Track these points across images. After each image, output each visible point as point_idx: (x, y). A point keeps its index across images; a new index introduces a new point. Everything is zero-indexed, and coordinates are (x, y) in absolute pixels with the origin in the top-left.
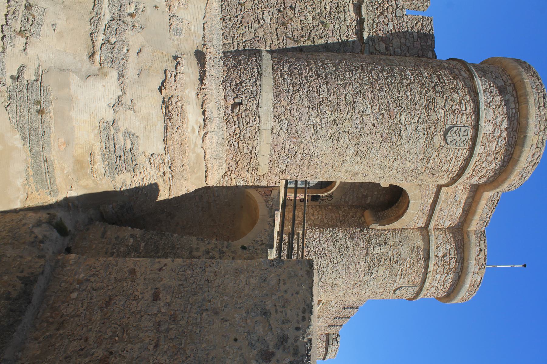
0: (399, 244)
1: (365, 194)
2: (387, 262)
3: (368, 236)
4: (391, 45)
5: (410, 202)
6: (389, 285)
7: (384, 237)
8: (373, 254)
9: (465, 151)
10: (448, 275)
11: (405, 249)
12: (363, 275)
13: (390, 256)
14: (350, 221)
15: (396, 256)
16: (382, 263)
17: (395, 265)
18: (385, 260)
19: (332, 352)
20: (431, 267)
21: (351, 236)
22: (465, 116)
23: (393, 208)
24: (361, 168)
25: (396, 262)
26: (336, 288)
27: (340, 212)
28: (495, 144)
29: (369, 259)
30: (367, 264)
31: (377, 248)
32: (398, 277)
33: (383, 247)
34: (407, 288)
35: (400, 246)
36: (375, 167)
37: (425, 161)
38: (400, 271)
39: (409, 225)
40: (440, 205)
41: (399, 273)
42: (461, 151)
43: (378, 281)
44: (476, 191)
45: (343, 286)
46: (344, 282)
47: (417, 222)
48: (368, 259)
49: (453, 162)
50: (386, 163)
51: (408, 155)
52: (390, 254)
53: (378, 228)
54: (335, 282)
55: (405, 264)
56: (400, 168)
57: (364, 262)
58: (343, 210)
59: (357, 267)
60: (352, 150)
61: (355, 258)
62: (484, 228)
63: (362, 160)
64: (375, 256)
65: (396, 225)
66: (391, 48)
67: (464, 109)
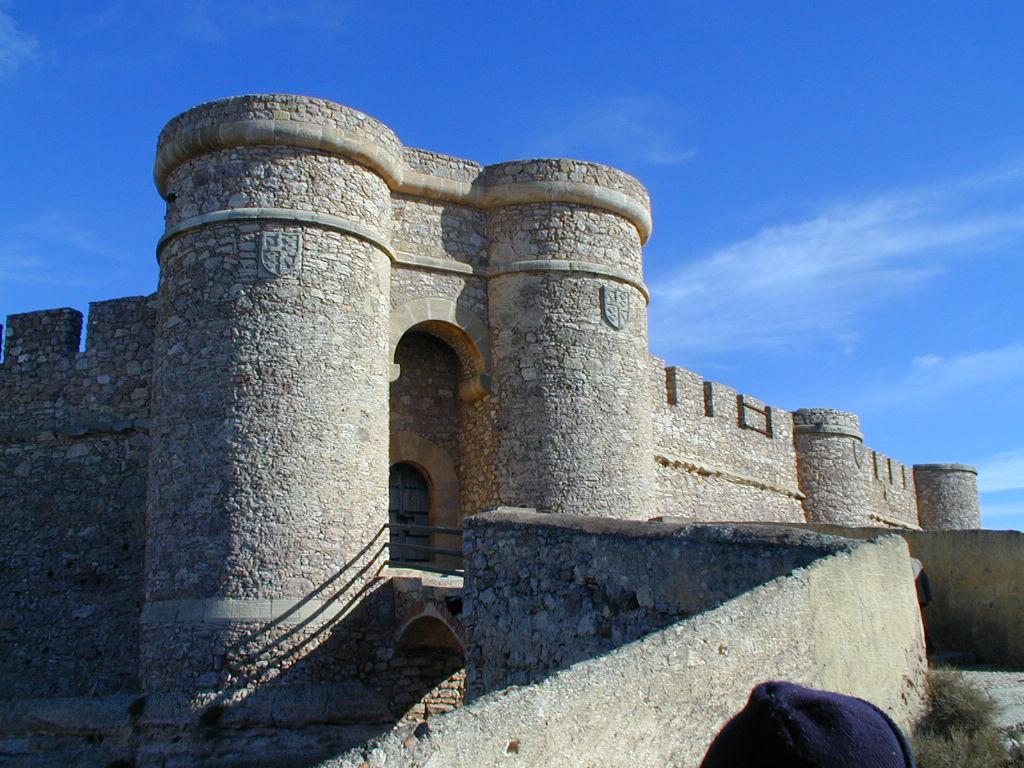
4: (136, 378)
5: (430, 318)
9: (307, 237)
10: (577, 229)
14: (481, 430)
16: (556, 363)
19: (837, 424)
22: (243, 246)
23: (453, 346)
24: (346, 425)
27: (468, 449)
28: (295, 184)
32: (585, 326)
34: (607, 307)
36: (345, 400)
38: (569, 325)
40: (435, 260)
41: (575, 326)
42: (309, 246)
46: (599, 434)
49: (332, 257)
50: (334, 380)
51: (318, 343)
54: (601, 452)
56: (346, 351)
58: (465, 444)
59: (565, 410)
60: (312, 448)
63: (331, 427)
66: (142, 377)
67: (228, 249)
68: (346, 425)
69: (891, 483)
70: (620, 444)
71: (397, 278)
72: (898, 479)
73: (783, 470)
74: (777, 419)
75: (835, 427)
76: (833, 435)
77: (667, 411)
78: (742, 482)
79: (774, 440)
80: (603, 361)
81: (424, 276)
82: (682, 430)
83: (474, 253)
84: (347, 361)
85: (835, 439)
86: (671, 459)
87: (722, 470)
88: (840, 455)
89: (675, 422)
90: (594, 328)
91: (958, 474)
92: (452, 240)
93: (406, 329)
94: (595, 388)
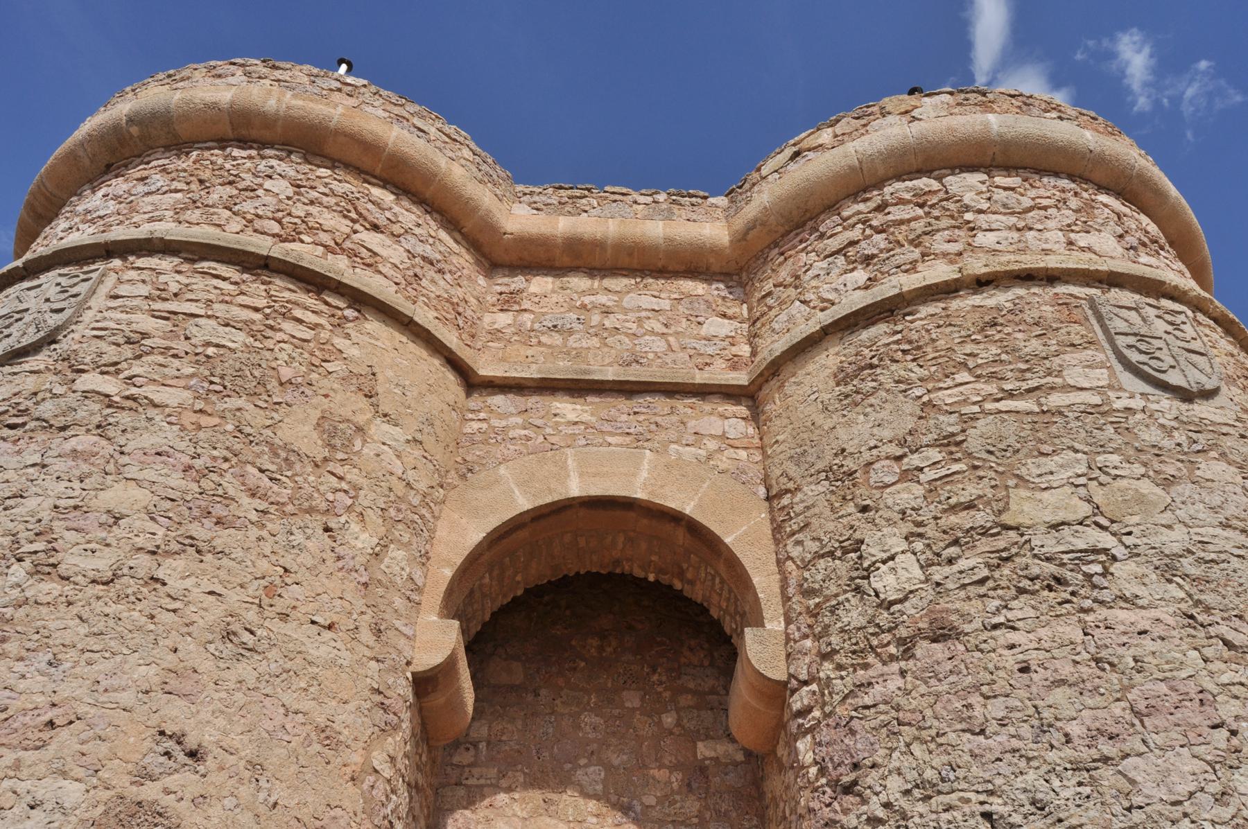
0: (841, 478)
1: (676, 778)
2: (970, 491)
3: (827, 669)
6: (1151, 435)
7: (816, 576)
8: (929, 593)
11: (858, 431)
12: (1121, 615)
13: (919, 490)
15: (915, 460)
16: (981, 518)
17: (974, 443)
18: (953, 509)
20: (939, 272)
21: (848, 789)
23: (697, 593)
25: (949, 442)
29: (974, 607)
30: (1021, 609)
31: (886, 582)
32: (1056, 400)
33: (873, 551)
35: (850, 464)
37: (125, 418)
39: (738, 474)
43: (1141, 499)
44: (502, 257)
47: (712, 445)
48: (974, 612)
52: (908, 495)
53: (775, 624)
55: (946, 397)
57: (1013, 637)
59: (1066, 670)
61: (997, 709)
62: (711, 200)
64: (938, 573)
65: (743, 532)
68: (43, 790)
71: (482, 415)
80: (1168, 482)
81: (567, 408)
83: (710, 350)
84: (144, 561)
90: (1097, 400)
92: (653, 333)
93: (494, 521)
94: (1168, 570)
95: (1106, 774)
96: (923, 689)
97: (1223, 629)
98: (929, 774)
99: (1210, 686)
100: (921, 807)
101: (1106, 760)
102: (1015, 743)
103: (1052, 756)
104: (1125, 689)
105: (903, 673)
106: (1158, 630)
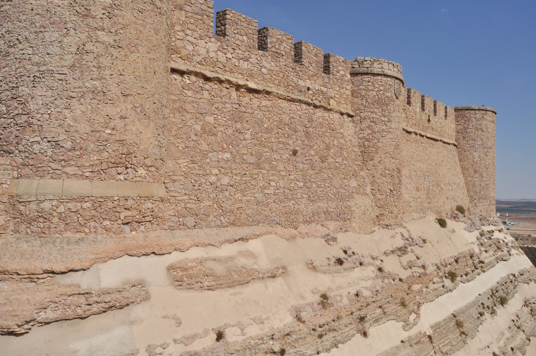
26: (89, 47)
45: (83, 36)
46: (72, 32)
54: (74, 50)
59: (40, 12)
61: (24, 17)
69: (435, 115)
70: (97, 44)
72: (441, 112)
73: (337, 96)
74: (336, 62)
75: (380, 70)
76: (378, 75)
77: (213, 40)
78: (293, 100)
79: (331, 76)
82: (229, 56)
85: (379, 78)
86: (209, 74)
87: (274, 89)
88: (382, 88)
89: (221, 49)
91: (483, 112)
95: (41, 34)
96: (12, 10)
97: (77, 8)
98: (10, 29)
99: (68, 20)
100: (7, 36)
101: (41, 32)
102: (26, 26)
103: (32, 29)
104: (50, 18)
105: (10, 5)
106: (62, 6)
